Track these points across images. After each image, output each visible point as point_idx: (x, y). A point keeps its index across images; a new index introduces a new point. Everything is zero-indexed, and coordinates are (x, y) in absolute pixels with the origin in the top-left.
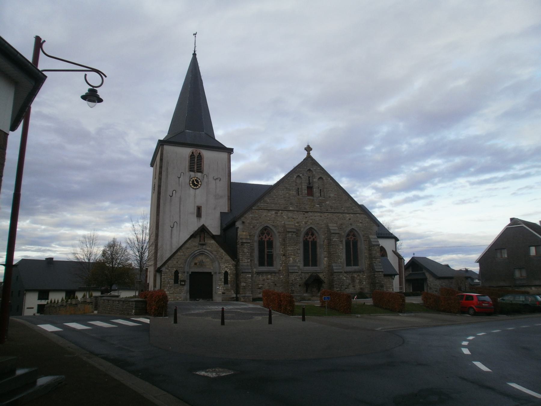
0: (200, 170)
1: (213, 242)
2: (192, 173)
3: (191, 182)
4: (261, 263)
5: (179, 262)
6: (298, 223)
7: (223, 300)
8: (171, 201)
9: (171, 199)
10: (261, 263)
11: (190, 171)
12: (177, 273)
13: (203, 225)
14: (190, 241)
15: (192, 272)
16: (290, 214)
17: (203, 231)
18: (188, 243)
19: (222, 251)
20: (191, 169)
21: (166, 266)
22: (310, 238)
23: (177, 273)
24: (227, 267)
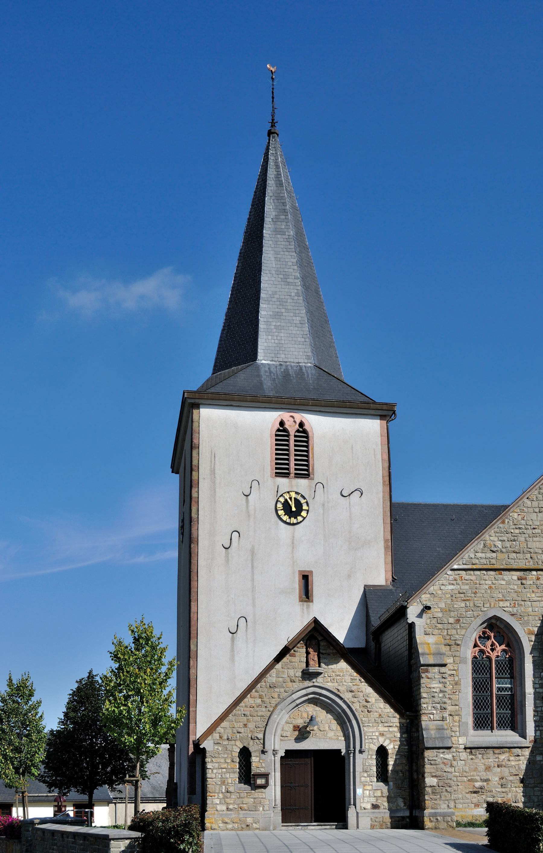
0: (304, 472)
1: (343, 665)
2: (282, 481)
3: (280, 506)
4: (482, 722)
5: (251, 726)
7: (372, 827)
8: (227, 561)
9: (227, 556)
10: (482, 722)
12: (245, 754)
13: (316, 621)
14: (279, 666)
15: (287, 752)
17: (316, 637)
18: (273, 672)
19: (369, 690)
21: (216, 736)
23: (245, 754)
24: (382, 735)
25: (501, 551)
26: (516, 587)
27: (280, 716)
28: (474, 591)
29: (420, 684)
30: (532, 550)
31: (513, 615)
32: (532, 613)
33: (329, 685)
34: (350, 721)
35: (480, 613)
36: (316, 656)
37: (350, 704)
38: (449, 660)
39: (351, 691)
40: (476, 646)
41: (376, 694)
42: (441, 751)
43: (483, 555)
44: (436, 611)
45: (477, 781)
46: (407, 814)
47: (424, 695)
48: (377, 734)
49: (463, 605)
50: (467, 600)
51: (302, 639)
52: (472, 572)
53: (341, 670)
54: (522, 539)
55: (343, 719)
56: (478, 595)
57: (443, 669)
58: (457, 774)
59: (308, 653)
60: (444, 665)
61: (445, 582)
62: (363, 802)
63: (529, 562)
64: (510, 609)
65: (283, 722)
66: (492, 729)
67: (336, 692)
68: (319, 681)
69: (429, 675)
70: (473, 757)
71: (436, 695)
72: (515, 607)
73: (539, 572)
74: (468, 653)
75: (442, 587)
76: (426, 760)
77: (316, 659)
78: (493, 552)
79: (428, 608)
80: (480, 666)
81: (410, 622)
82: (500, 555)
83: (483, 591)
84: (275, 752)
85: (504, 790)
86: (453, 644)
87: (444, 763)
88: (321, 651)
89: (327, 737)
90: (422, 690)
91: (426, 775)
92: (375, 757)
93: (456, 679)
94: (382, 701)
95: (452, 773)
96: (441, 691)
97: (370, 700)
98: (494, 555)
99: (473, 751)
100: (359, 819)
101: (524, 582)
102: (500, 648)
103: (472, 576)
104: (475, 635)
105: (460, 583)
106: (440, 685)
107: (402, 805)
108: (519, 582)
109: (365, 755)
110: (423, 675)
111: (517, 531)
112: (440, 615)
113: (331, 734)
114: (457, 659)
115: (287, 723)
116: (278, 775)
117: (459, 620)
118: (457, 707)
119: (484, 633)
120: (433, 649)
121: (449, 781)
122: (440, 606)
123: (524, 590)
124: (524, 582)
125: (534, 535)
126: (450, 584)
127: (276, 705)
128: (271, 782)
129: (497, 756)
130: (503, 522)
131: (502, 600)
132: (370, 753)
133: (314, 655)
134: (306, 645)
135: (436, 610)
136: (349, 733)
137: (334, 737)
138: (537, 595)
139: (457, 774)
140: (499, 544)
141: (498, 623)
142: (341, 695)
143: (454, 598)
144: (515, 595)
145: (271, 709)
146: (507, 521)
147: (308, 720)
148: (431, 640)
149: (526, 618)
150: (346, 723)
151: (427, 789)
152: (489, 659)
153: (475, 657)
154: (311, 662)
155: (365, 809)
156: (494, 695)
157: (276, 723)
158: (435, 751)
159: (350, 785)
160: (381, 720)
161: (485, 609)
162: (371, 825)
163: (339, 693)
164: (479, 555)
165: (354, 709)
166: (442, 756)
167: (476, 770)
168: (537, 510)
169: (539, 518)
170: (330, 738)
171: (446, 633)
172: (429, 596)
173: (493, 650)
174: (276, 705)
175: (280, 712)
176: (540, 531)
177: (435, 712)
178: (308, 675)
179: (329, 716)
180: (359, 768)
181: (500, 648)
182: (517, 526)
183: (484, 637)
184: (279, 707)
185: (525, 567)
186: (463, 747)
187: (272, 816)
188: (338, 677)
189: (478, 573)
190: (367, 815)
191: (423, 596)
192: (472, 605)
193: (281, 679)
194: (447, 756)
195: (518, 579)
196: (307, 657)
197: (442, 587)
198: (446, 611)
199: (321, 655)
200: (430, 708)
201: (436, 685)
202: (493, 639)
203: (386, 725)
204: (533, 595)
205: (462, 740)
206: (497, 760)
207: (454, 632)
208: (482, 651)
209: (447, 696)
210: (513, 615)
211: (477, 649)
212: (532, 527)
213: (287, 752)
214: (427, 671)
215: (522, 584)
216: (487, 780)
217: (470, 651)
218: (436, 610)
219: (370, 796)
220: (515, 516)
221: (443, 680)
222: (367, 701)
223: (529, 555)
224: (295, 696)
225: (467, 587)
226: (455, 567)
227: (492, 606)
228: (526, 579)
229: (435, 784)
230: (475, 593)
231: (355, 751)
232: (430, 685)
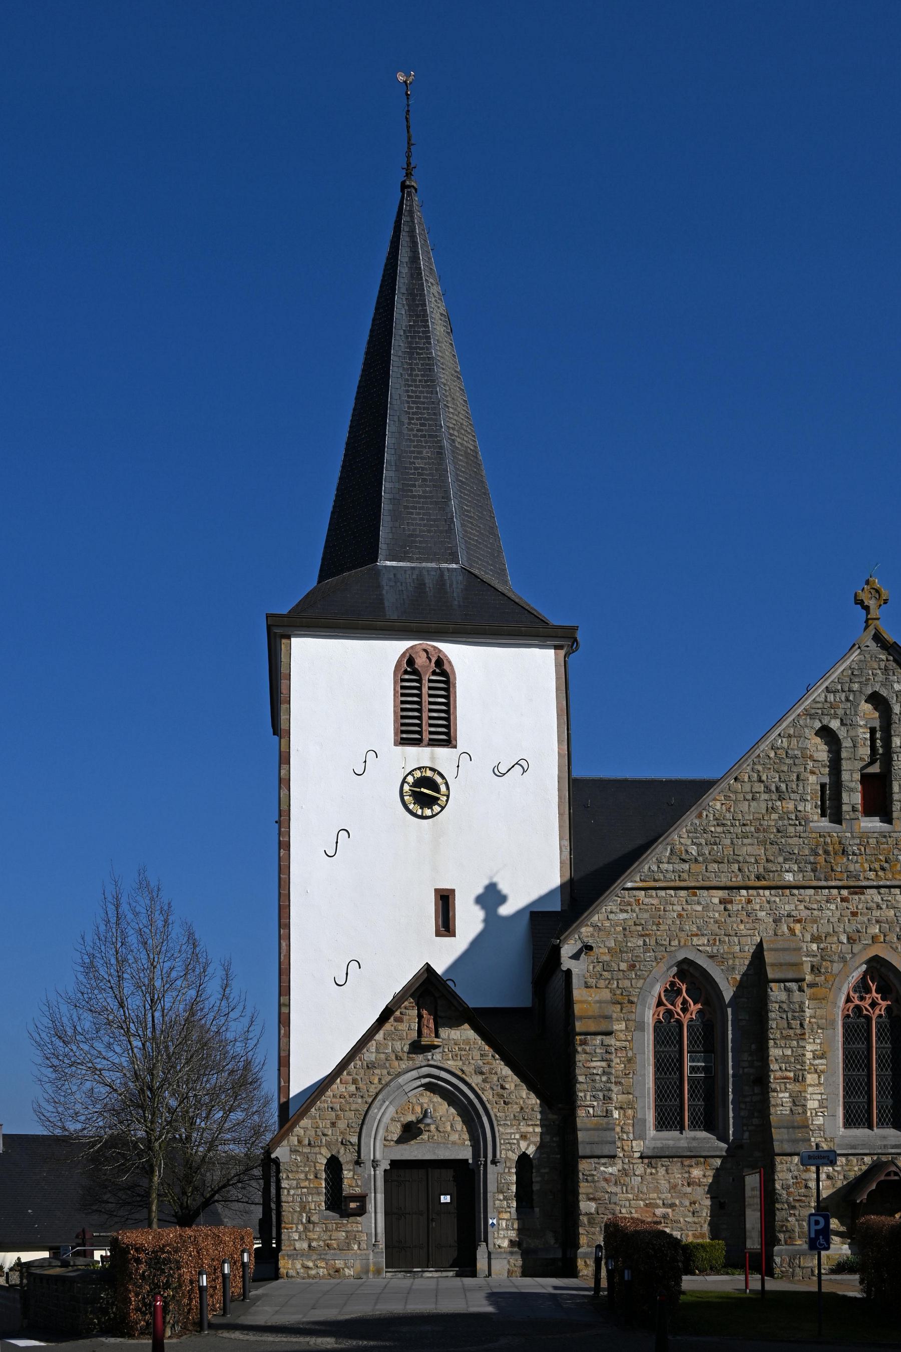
1: (466, 1033)
6: (815, 939)
11: (402, 741)
15: (393, 1163)
16: (787, 905)
19: (507, 1071)
20: (408, 734)
22: (874, 1004)
25: (696, 860)
26: (717, 915)
27: (382, 1110)
28: (656, 921)
29: (575, 1063)
30: (741, 859)
31: (711, 957)
32: (739, 955)
33: (450, 1064)
34: (479, 1117)
35: (665, 954)
36: (431, 1021)
37: (480, 1092)
38: (619, 1026)
39: (482, 1073)
40: (660, 1003)
41: (515, 1077)
42: (603, 1161)
43: (670, 867)
44: (601, 951)
45: (658, 1207)
46: (559, 1255)
47: (581, 1079)
48: (517, 1136)
49: (641, 943)
50: (647, 935)
51: (412, 996)
52: (653, 893)
53: (467, 1042)
54: (728, 842)
55: (471, 1115)
56: (662, 927)
57: (609, 1040)
58: (630, 1196)
59: (420, 1016)
60: (609, 1033)
61: (614, 908)
62: (498, 1238)
63: (737, 876)
64: (708, 949)
65: (387, 1119)
66: (682, 1129)
67: (460, 1073)
68: (436, 1057)
69: (588, 1048)
70: (654, 1171)
71: (598, 1078)
72: (714, 944)
73: (750, 891)
74: (649, 1016)
75: (611, 916)
76: (581, 1176)
77: (432, 1025)
78: (684, 861)
79: (589, 948)
80: (667, 1033)
81: (564, 969)
82: (695, 868)
83: (670, 922)
84: (375, 1164)
85: (696, 1220)
86: (625, 1001)
87: (606, 1180)
88: (439, 1013)
89: (449, 1140)
90: (578, 1071)
91: (581, 1197)
92: (514, 1170)
93: (630, 1054)
94: (525, 1087)
95: (616, 1194)
96: (604, 1073)
97: (507, 1086)
98: (686, 866)
99: (653, 1161)
100: (493, 1262)
101: (729, 906)
102: (694, 1008)
103: (652, 899)
104: (658, 989)
105: (637, 909)
106: (604, 1064)
107: (552, 1241)
108: (722, 907)
109: (500, 1168)
110: (579, 1049)
111: (719, 829)
112: (607, 958)
113: (454, 1137)
114: (631, 1024)
115: (393, 1120)
116: (380, 1197)
117: (634, 966)
118: (631, 1096)
119: (673, 984)
120: (595, 1009)
121: (612, 1206)
122: (607, 944)
123: (729, 920)
124: (729, 906)
126: (621, 910)
127: (377, 1094)
128: (370, 1207)
129: (687, 1169)
130: (700, 816)
131: (697, 935)
132: (508, 1165)
133: (429, 1021)
134: (417, 1004)
135: (601, 950)
136: (478, 1136)
137: (458, 1141)
138: (748, 926)
139: (630, 1196)
140: (694, 850)
141: (691, 970)
142: (467, 1079)
143: (627, 932)
144: (715, 927)
145: (370, 1100)
146: (705, 814)
147: (421, 1116)
148: (593, 996)
149: (731, 962)
150: (474, 1120)
151: (581, 1217)
152: (679, 1023)
153: (659, 1021)
154: (425, 1031)
155: (499, 1246)
156: (686, 1078)
157: (377, 1121)
158: (592, 1160)
159: (480, 1212)
160: (522, 1115)
161: (673, 949)
162: (509, 1271)
163: (464, 1076)
164: (664, 866)
165: (485, 1099)
166: (602, 1169)
167: (657, 1190)
168: (749, 797)
169: (752, 810)
170: (454, 1143)
171: (615, 986)
172: (591, 929)
173: (685, 1010)
174: (377, 1094)
175: (381, 1105)
176: (753, 829)
177: (595, 1103)
178: (417, 1048)
179: (452, 1110)
180: (492, 1187)
181: (694, 1008)
183: (672, 992)
184: (380, 1097)
185: (729, 884)
186: (637, 1155)
187: (371, 1257)
188: (463, 1053)
189: (662, 893)
190: (504, 1256)
191: (583, 930)
192: (653, 942)
193: (383, 1056)
194: (610, 1170)
195: (721, 902)
196: (419, 1023)
197: (611, 916)
198: (617, 952)
199: (439, 1020)
200: (588, 1098)
201: (598, 1065)
202: (684, 994)
203: (530, 1123)
204: (742, 927)
205: (638, 1146)
206: (686, 1175)
207: (627, 983)
208: (669, 1013)
209: (613, 1080)
210: (711, 957)
211: (662, 1009)
213: (393, 1163)
214: (584, 1043)
215: (725, 909)
216: (672, 1206)
217: (651, 1012)
218: (601, 950)
219: (507, 1229)
220: (718, 806)
221: (608, 1056)
222: (503, 1088)
223: (736, 866)
224: (401, 1080)
225: (646, 915)
226: (629, 885)
227: (682, 944)
228: (731, 902)
229: (593, 1210)
230: (658, 924)
231: (486, 1161)
232: (589, 1062)
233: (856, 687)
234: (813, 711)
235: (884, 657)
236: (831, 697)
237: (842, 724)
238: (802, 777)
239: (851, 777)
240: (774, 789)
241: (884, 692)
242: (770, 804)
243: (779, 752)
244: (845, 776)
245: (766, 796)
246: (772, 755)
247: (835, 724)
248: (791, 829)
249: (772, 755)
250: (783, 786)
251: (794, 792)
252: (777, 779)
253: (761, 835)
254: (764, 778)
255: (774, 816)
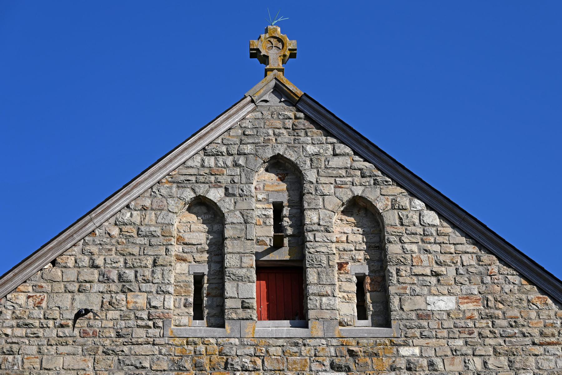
125: (62, 341)
168: (75, 287)
182: (21, 322)
212: (58, 322)
220: (22, 299)
233: (248, 149)
234: (183, 178)
235: (291, 115)
236: (211, 161)
237: (227, 194)
238: (160, 262)
239: (241, 262)
240: (114, 275)
241: (291, 156)
242: (107, 297)
243: (125, 228)
244: (230, 261)
245: (102, 287)
246: (115, 231)
247: (215, 195)
248: (141, 333)
249: (115, 231)
250: (130, 274)
251: (146, 281)
252: (121, 264)
253: (90, 341)
254: (99, 261)
255: (112, 314)
